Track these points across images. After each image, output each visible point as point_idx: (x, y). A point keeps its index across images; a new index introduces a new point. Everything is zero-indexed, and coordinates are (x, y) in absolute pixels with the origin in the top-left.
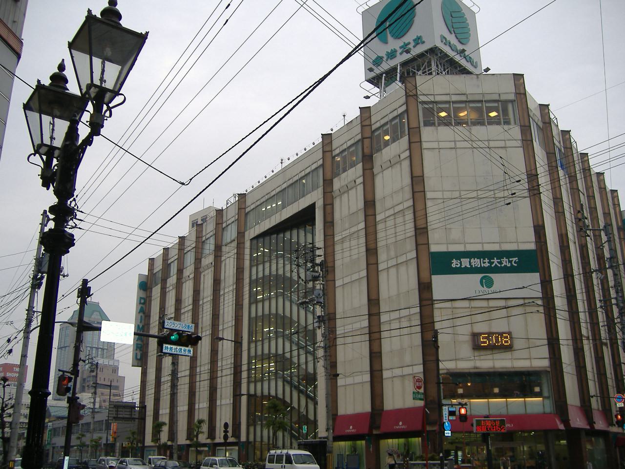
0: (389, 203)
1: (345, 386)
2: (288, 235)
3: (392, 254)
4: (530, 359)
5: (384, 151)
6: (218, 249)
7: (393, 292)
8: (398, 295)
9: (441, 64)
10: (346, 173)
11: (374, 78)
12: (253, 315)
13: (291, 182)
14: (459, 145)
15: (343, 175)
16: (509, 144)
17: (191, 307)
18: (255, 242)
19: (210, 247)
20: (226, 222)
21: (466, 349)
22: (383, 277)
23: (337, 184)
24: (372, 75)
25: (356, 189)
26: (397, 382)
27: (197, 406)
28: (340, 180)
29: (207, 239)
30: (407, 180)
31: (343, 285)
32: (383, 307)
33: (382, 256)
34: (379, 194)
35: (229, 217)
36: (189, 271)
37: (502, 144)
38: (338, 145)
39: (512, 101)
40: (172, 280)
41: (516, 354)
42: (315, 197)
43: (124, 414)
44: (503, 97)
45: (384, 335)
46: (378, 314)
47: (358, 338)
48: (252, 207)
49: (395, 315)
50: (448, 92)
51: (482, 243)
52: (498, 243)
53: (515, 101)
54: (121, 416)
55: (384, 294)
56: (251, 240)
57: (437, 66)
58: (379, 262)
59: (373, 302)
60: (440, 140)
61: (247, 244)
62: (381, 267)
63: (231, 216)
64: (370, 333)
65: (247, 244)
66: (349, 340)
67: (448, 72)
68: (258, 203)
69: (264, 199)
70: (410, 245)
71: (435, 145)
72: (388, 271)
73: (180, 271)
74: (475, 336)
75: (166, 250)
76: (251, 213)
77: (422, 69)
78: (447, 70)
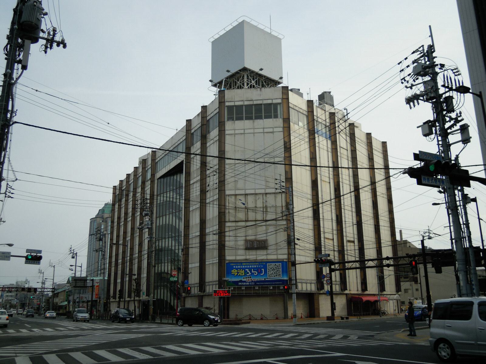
2: (175, 177)
4: (277, 254)
6: (144, 183)
7: (211, 217)
8: (213, 218)
14: (246, 131)
16: (275, 130)
18: (159, 180)
26: (211, 266)
27: (142, 277)
37: (271, 130)
39: (280, 104)
41: (269, 251)
43: (79, 284)
44: (275, 101)
48: (159, 159)
53: (281, 103)
54: (78, 285)
56: (158, 179)
60: (236, 129)
61: (156, 181)
65: (156, 181)
78: (255, 80)
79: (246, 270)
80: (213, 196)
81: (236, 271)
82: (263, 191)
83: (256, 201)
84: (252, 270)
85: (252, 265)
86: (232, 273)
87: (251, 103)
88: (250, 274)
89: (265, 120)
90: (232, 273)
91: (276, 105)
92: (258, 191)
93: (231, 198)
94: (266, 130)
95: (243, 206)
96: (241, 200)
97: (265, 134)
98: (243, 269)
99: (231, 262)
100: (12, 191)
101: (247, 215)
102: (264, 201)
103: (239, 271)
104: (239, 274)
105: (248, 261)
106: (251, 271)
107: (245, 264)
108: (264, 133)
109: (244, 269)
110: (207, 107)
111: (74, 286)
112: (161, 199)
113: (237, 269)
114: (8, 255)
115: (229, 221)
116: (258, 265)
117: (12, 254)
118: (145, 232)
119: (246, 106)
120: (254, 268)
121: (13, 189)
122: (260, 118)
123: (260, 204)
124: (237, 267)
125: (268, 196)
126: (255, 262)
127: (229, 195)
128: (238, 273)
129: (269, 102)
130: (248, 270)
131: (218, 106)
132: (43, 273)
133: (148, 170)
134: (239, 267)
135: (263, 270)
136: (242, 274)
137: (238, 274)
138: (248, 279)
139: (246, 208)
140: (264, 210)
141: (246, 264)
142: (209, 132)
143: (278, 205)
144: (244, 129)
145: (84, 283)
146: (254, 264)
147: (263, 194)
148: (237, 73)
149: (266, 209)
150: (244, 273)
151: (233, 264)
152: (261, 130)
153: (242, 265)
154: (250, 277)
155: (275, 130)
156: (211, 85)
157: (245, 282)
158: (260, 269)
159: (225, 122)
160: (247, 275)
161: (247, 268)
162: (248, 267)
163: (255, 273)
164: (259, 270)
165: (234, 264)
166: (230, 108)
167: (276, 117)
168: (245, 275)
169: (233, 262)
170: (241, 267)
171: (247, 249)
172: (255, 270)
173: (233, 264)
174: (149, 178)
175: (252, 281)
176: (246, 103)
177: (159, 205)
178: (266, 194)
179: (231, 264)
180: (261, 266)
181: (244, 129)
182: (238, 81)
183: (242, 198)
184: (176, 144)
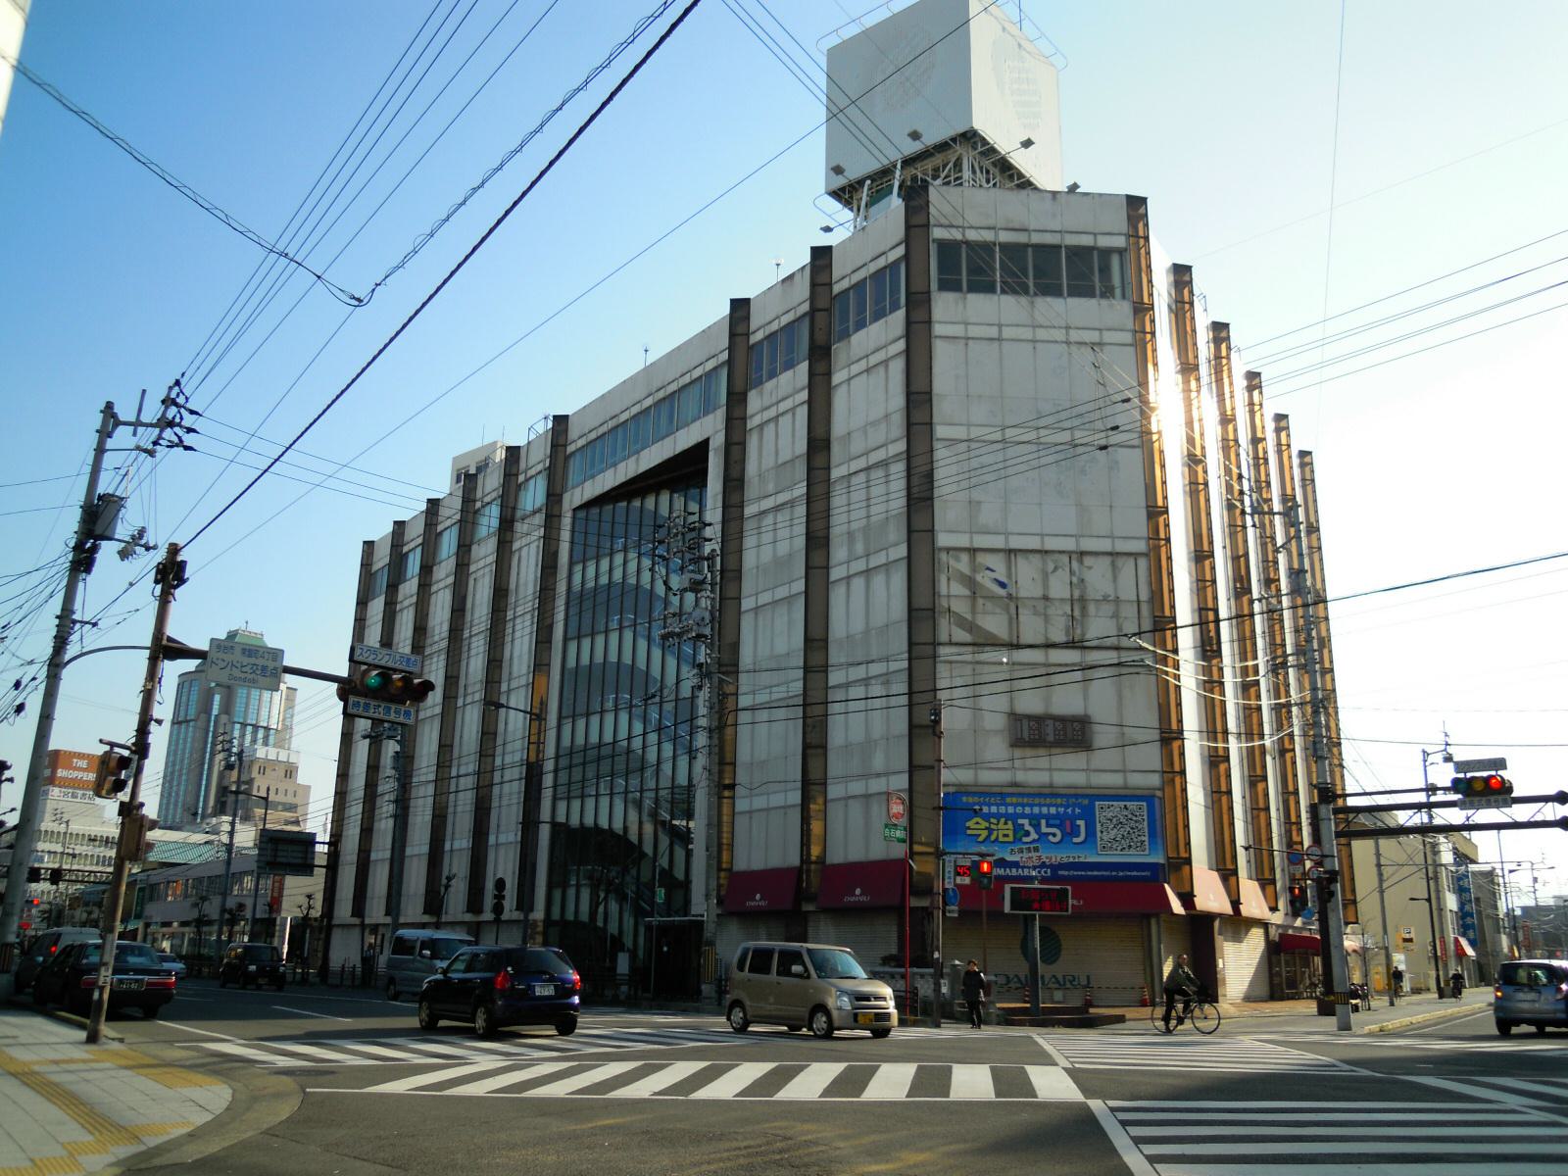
0: (857, 445)
1: (750, 812)
2: (650, 502)
3: (859, 548)
5: (853, 338)
6: (507, 524)
8: (867, 631)
9: (981, 168)
10: (775, 380)
11: (843, 189)
12: (571, 663)
13: (661, 394)
14: (1007, 333)
15: (769, 385)
16: (1108, 337)
17: (444, 644)
18: (581, 514)
19: (490, 519)
20: (526, 472)
21: (997, 748)
22: (837, 596)
23: (754, 402)
24: (840, 181)
25: (794, 414)
26: (856, 809)
27: (447, 847)
28: (761, 394)
29: (483, 507)
30: (898, 401)
31: (757, 608)
32: (836, 656)
33: (838, 553)
34: (838, 428)
35: (532, 461)
36: (444, 571)
37: (1094, 336)
38: (762, 322)
39: (1121, 252)
40: (409, 588)
41: (1098, 759)
42: (710, 427)
44: (1104, 242)
45: (834, 708)
46: (825, 669)
47: (781, 713)
48: (581, 443)
49: (859, 672)
50: (991, 222)
51: (1042, 535)
52: (1072, 536)
53: (1126, 250)
55: (838, 628)
56: (574, 510)
57: (974, 172)
58: (832, 563)
59: (816, 642)
60: (971, 321)
61: (567, 521)
62: (836, 573)
63: (537, 460)
64: (805, 705)
65: (567, 521)
66: (764, 715)
67: (994, 185)
68: (593, 435)
69: (604, 429)
70: (897, 533)
71: (957, 330)
72: (848, 583)
73: (427, 569)
74: (1015, 717)
75: (399, 526)
76: (578, 455)
77: (943, 175)
79: (1020, 821)
80: (868, 555)
81: (985, 824)
82: (1069, 545)
83: (1045, 576)
84: (1043, 822)
85: (1040, 805)
86: (969, 832)
87: (1022, 238)
88: (1036, 837)
89: (1070, 300)
90: (969, 832)
91: (1106, 253)
92: (1051, 544)
93: (958, 560)
94: (1075, 336)
95: (1002, 592)
96: (993, 571)
97: (1074, 348)
98: (1007, 817)
99: (963, 790)
100: (189, 420)
101: (1014, 621)
102: (1075, 580)
103: (993, 827)
104: (993, 838)
105: (1027, 790)
106: (1037, 827)
107: (1014, 800)
108: (1068, 343)
109: (1014, 818)
110: (834, 250)
111: (268, 863)
112: (590, 574)
113: (987, 817)
114: (271, 665)
115: (951, 643)
116: (1061, 805)
117: (288, 662)
118: (509, 691)
119: (1006, 248)
120: (1048, 817)
121: (192, 412)
122: (1056, 292)
123: (1059, 588)
124: (985, 809)
125: (1088, 561)
126: (1049, 793)
127: (948, 550)
128: (990, 831)
129: (1086, 241)
130: (1025, 822)
131: (901, 233)
132: (67, 822)
133: (527, 480)
134: (994, 809)
135: (1081, 823)
136: (1006, 836)
137: (990, 834)
138: (1026, 855)
139: (1010, 597)
140: (1077, 613)
141: (1020, 800)
142: (845, 335)
143: (1123, 597)
144: (1000, 326)
145: (306, 852)
146: (1048, 801)
147: (1070, 553)
148: (943, 147)
149: (1084, 609)
150: (1011, 833)
151: (971, 800)
152: (1060, 335)
153: (1006, 805)
154: (1036, 850)
155: (1108, 337)
156: (823, 191)
157: (1016, 865)
158: (1074, 818)
159: (928, 293)
160: (1025, 839)
161: (1024, 816)
162: (1027, 810)
163: (1054, 835)
164: (1068, 822)
165: (976, 799)
166: (948, 249)
167: (1107, 292)
168: (1017, 840)
169: (974, 789)
170: (1003, 810)
171: (1017, 743)
172: (1051, 822)
173: (971, 800)
174: (529, 508)
175: (1043, 865)
176: (1005, 237)
177: (579, 600)
178: (1082, 554)
179: (964, 799)
180: (1073, 811)
181: (1000, 326)
182: (935, 178)
183: (997, 563)
184: (673, 387)
